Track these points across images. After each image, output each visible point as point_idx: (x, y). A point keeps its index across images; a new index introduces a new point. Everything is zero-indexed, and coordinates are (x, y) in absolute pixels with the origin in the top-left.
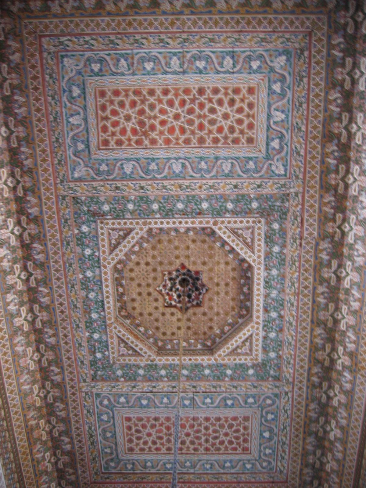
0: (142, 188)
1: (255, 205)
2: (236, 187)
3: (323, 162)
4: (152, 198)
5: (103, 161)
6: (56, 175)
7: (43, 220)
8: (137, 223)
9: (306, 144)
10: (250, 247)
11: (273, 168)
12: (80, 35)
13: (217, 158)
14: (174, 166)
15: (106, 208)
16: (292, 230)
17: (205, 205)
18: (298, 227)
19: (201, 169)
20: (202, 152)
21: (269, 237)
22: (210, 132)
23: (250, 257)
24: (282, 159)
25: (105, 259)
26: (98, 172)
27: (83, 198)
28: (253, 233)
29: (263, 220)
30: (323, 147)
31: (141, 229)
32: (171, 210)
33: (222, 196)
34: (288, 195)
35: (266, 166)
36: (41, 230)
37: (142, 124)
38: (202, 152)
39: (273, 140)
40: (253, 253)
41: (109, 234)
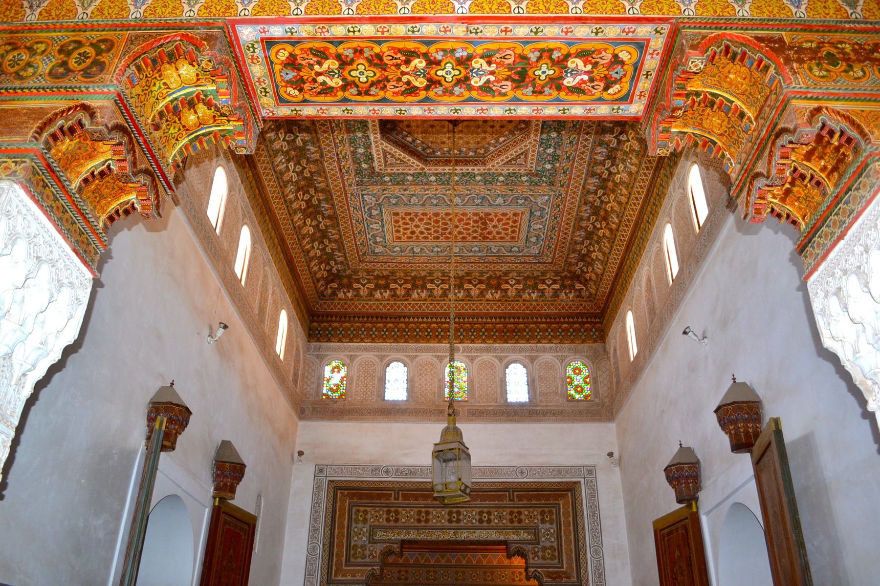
0: (488, 190)
1: (387, 179)
2: (405, 190)
3: (333, 205)
4: (480, 183)
5: (521, 205)
6: (564, 200)
7: (587, 175)
8: (497, 170)
9: (350, 213)
10: (385, 153)
11: (374, 199)
12: (523, 263)
13: (423, 205)
14: (460, 201)
15: (524, 179)
16: (349, 164)
17: (433, 178)
18: (344, 166)
19: (436, 199)
20: (436, 210)
21: (369, 159)
22: (430, 219)
23: (386, 147)
24: (367, 204)
25: (534, 146)
26: (526, 199)
27: (544, 184)
28: (386, 162)
29: (377, 170)
30: (335, 213)
31: (493, 166)
32: (465, 176)
33: (417, 184)
34: (357, 185)
35: (381, 200)
36: (591, 169)
37: (485, 223)
38: (436, 210)
39: (377, 214)
40: (383, 149)
41: (525, 162)
